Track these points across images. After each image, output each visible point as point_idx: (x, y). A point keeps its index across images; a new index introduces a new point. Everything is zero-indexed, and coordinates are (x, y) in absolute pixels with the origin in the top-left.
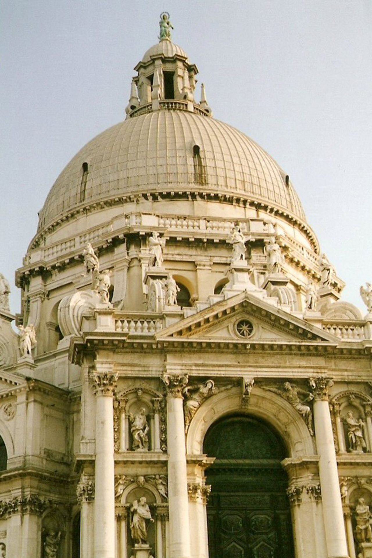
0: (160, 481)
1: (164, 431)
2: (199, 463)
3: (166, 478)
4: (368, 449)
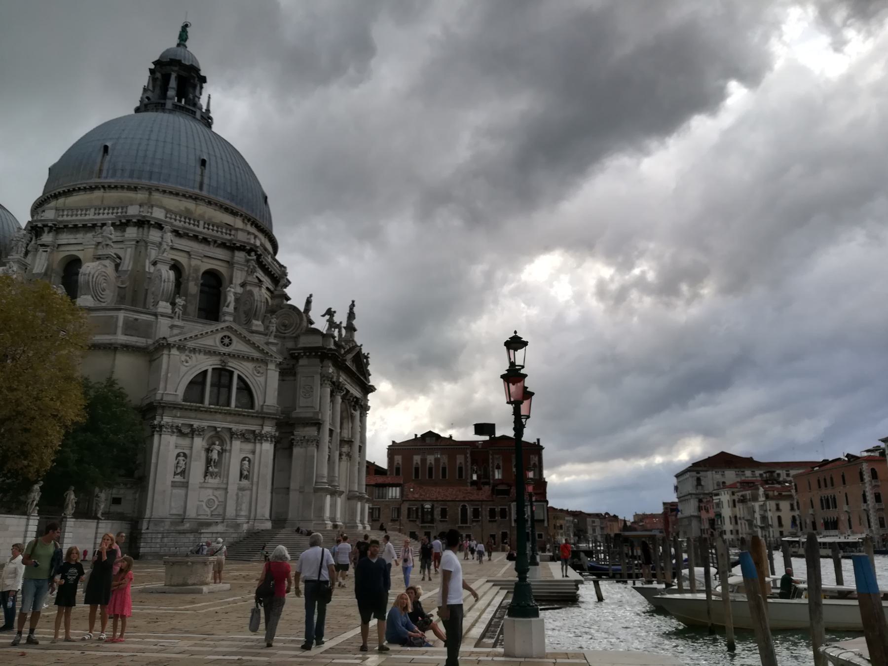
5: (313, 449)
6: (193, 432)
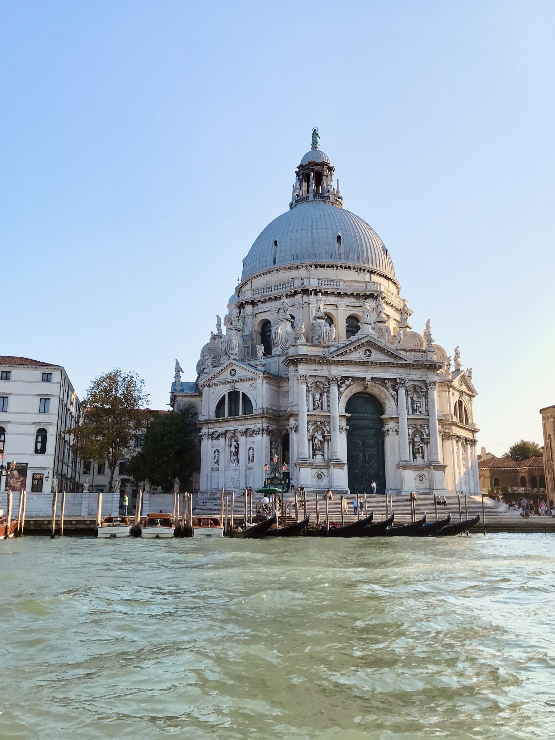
0: (327, 424)
1: (328, 401)
2: (344, 416)
4: (422, 412)
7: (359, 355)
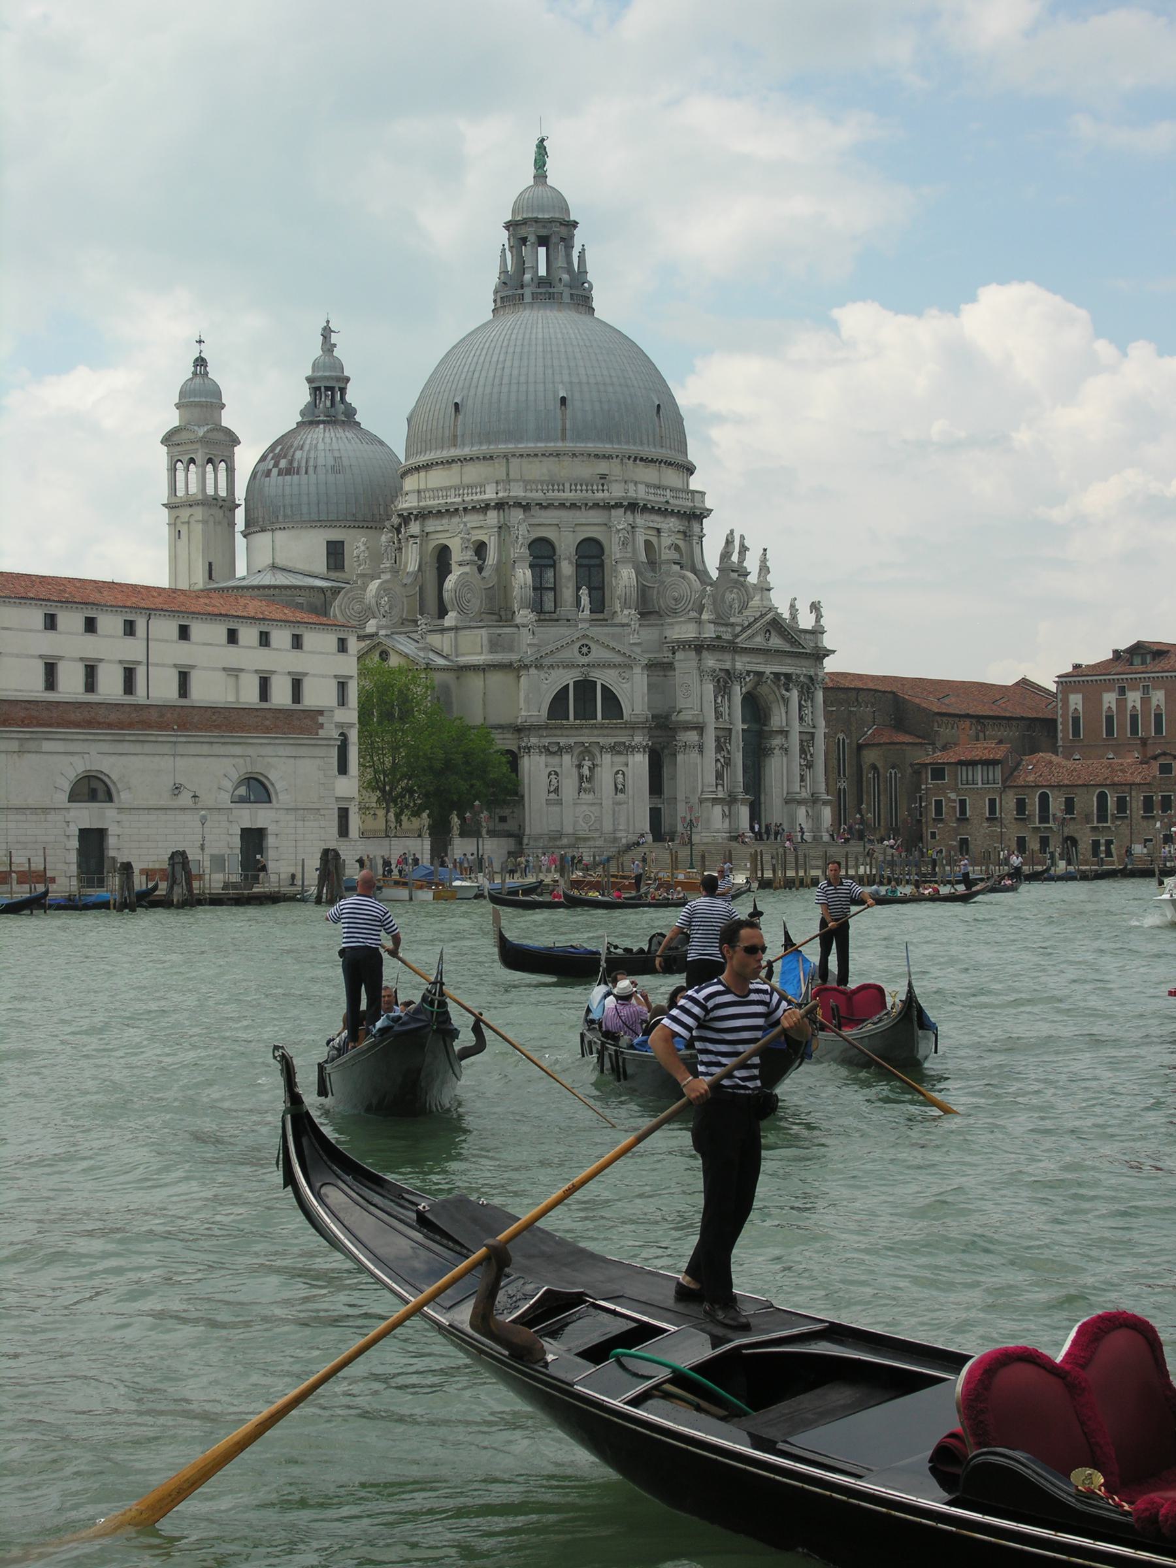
3: (730, 740)
5: (694, 755)
6: (561, 751)
7: (759, 641)
